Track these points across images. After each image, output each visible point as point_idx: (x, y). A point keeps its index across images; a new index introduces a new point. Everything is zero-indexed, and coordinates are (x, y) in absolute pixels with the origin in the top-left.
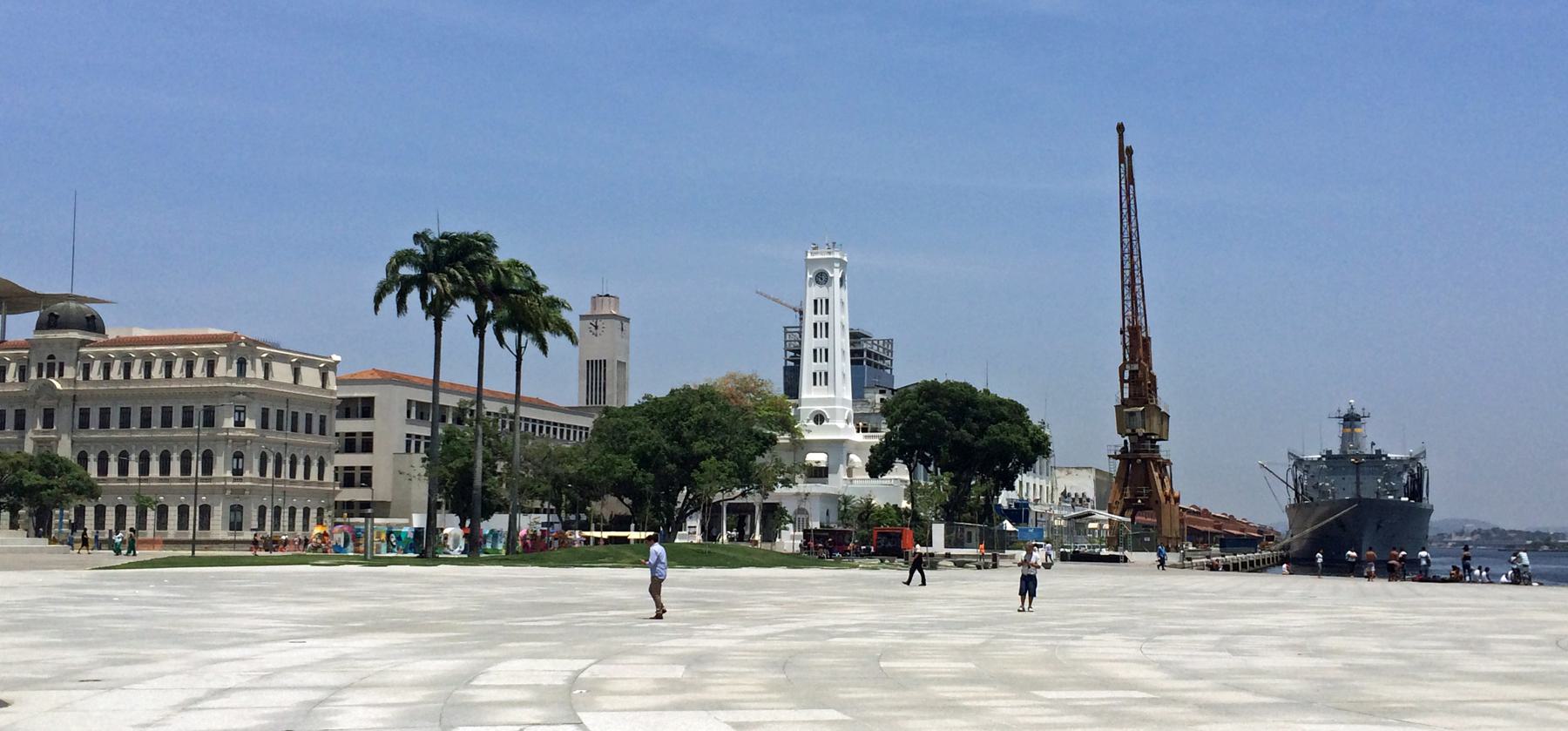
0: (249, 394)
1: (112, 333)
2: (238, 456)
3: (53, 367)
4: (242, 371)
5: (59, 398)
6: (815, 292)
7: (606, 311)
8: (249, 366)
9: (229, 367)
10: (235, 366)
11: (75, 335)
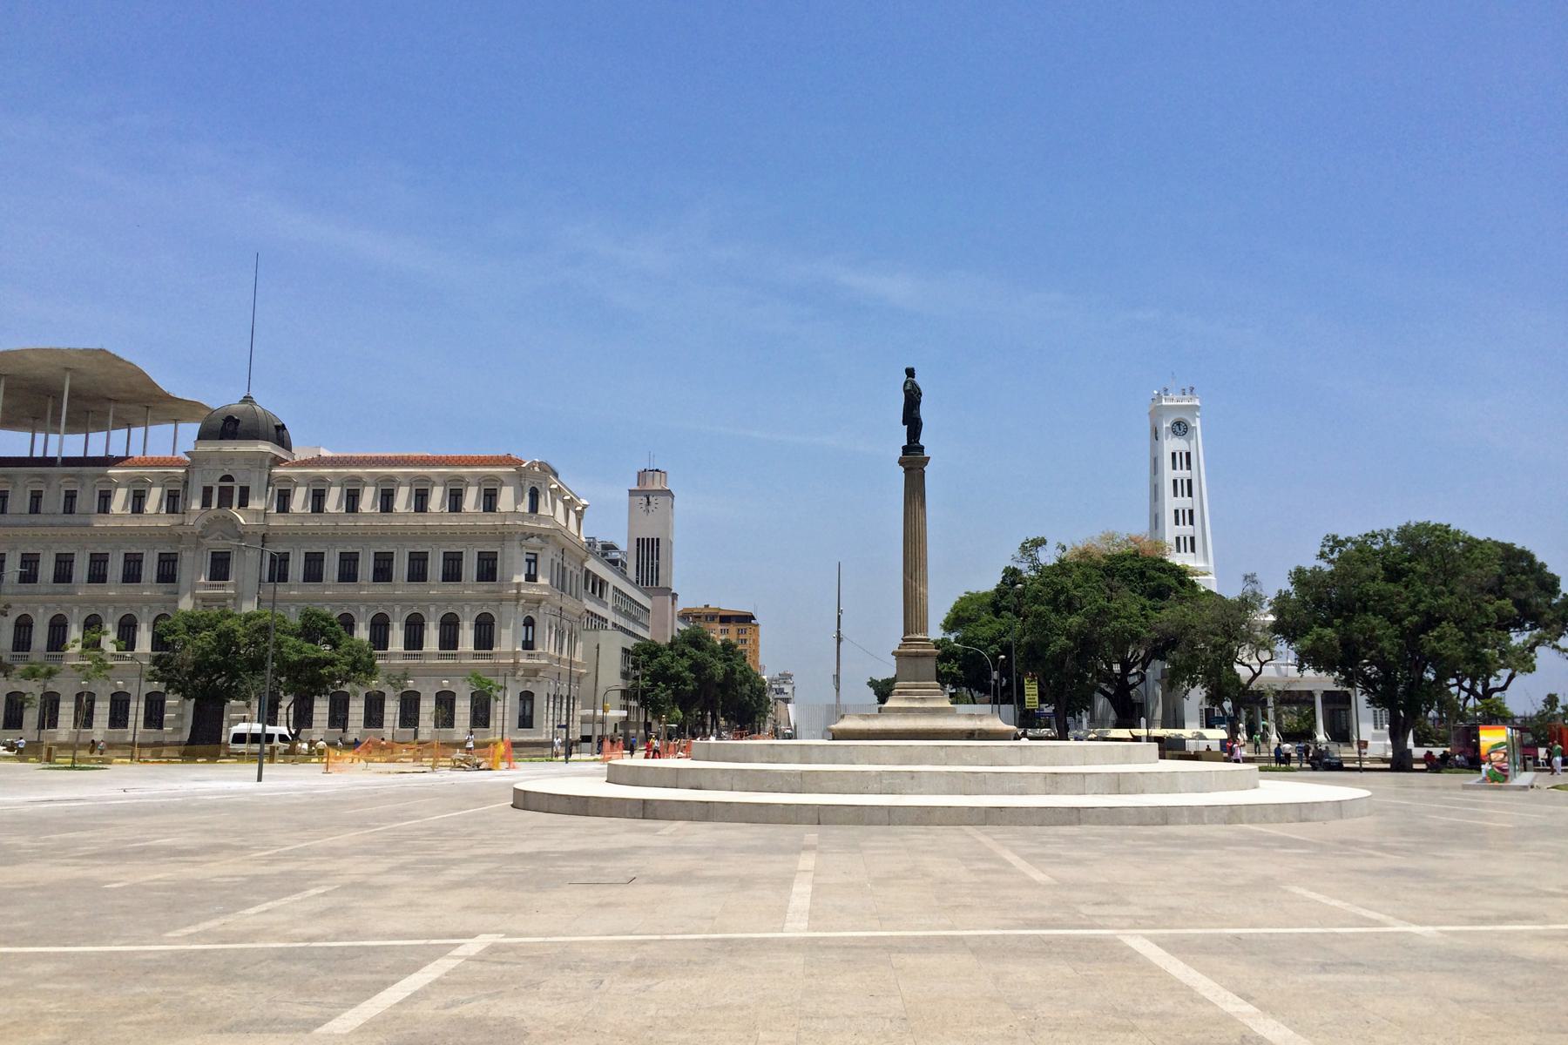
0: (544, 537)
1: (300, 452)
2: (529, 623)
3: (229, 493)
4: (534, 508)
5: (241, 537)
6: (1171, 444)
9: (518, 500)
11: (265, 447)
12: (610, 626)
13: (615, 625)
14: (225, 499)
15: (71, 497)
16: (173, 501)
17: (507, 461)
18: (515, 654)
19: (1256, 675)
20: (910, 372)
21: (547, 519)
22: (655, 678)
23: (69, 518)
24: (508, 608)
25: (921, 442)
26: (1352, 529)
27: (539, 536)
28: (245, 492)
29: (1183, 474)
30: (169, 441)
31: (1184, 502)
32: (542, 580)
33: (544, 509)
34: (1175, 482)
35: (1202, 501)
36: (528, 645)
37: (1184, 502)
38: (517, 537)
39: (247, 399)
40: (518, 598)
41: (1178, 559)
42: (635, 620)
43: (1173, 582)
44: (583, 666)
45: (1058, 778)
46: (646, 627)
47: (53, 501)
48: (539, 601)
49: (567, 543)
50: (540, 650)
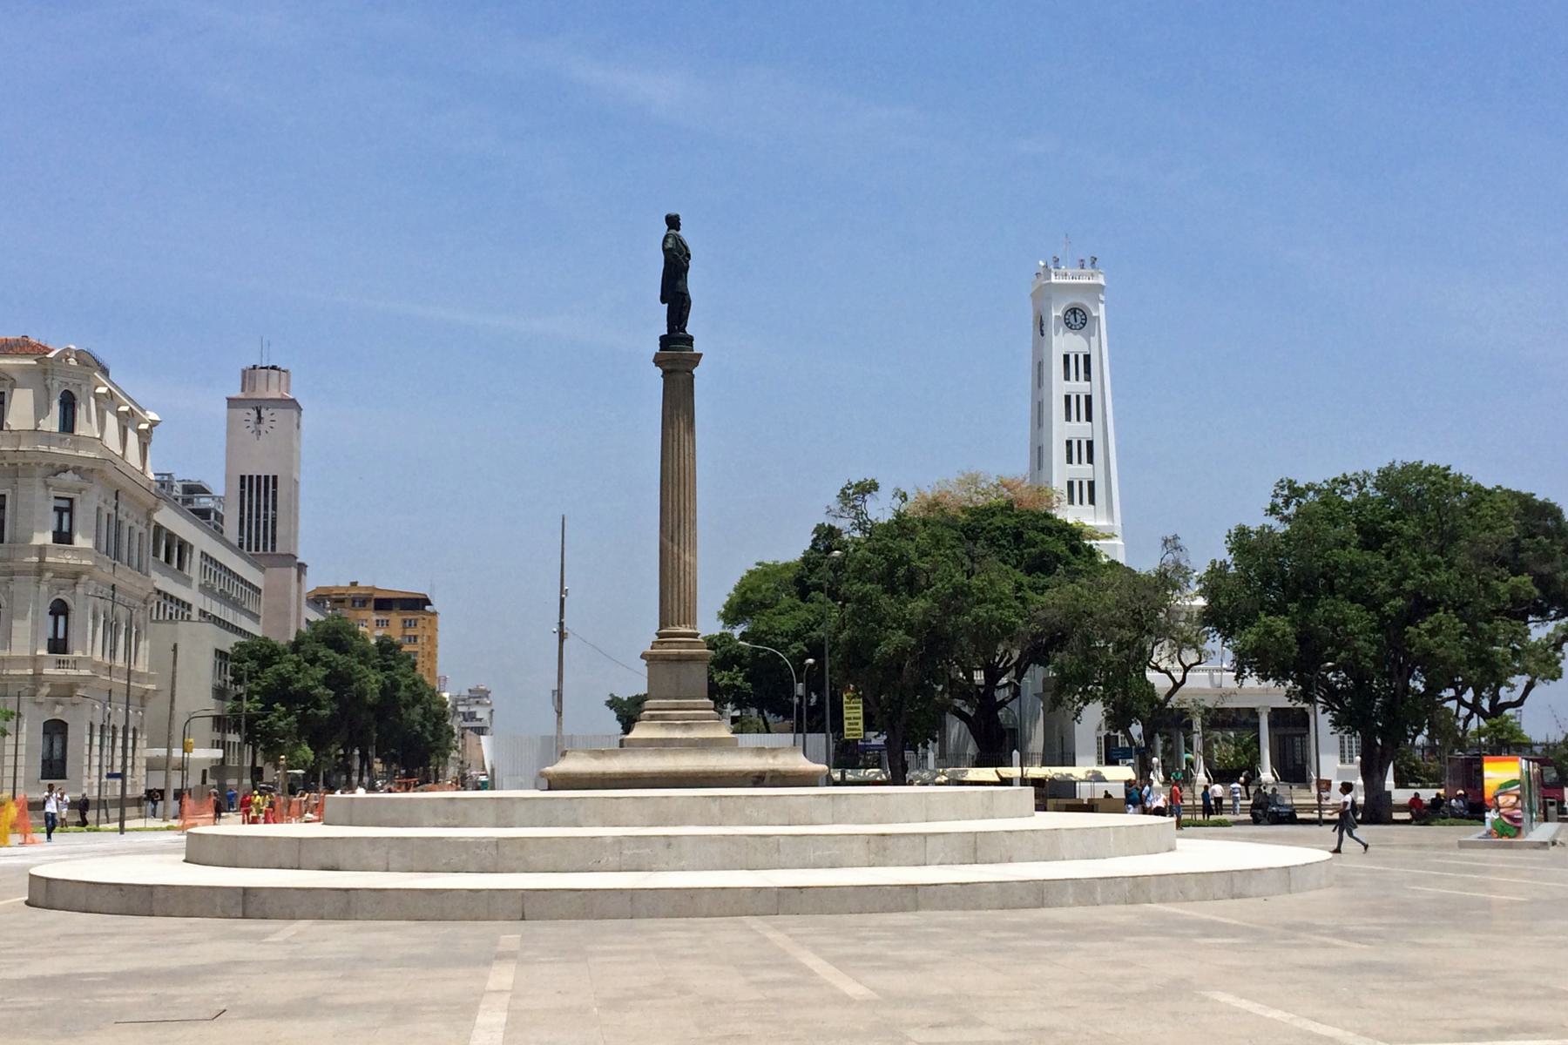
0: (85, 471)
2: (60, 609)
4: (68, 424)
6: (1064, 342)
7: (274, 394)
8: (81, 414)
9: (41, 411)
10: (56, 408)
12: (195, 615)
13: (203, 613)
17: (20, 347)
18: (36, 659)
19: (1177, 686)
20: (673, 222)
21: (90, 442)
22: (269, 697)
24: (22, 586)
25: (689, 330)
26: (1315, 472)
27: (76, 470)
29: (1079, 387)
31: (1079, 430)
32: (80, 541)
33: (85, 426)
34: (1068, 398)
35: (1106, 429)
36: (58, 646)
37: (1079, 430)
38: (39, 471)
40: (40, 570)
41: (1070, 514)
42: (236, 605)
43: (1062, 548)
44: (150, 679)
45: (889, 842)
46: (255, 617)
48: (76, 575)
49: (122, 482)
50: (78, 654)
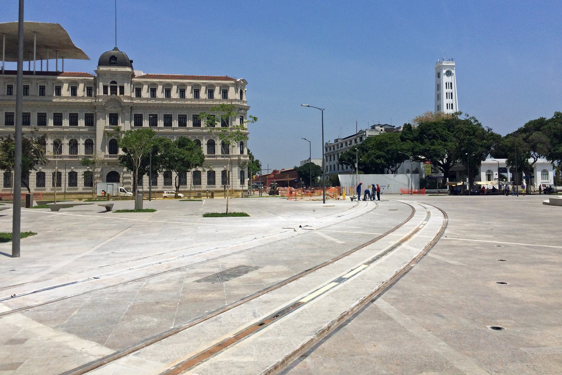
5: (121, 107)
14: (114, 90)
15: (42, 89)
16: (90, 91)
17: (227, 78)
23: (42, 98)
28: (122, 88)
30: (90, 67)
39: (116, 49)
47: (34, 90)
